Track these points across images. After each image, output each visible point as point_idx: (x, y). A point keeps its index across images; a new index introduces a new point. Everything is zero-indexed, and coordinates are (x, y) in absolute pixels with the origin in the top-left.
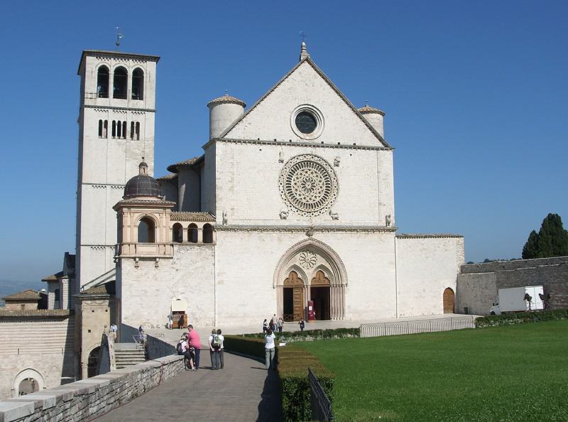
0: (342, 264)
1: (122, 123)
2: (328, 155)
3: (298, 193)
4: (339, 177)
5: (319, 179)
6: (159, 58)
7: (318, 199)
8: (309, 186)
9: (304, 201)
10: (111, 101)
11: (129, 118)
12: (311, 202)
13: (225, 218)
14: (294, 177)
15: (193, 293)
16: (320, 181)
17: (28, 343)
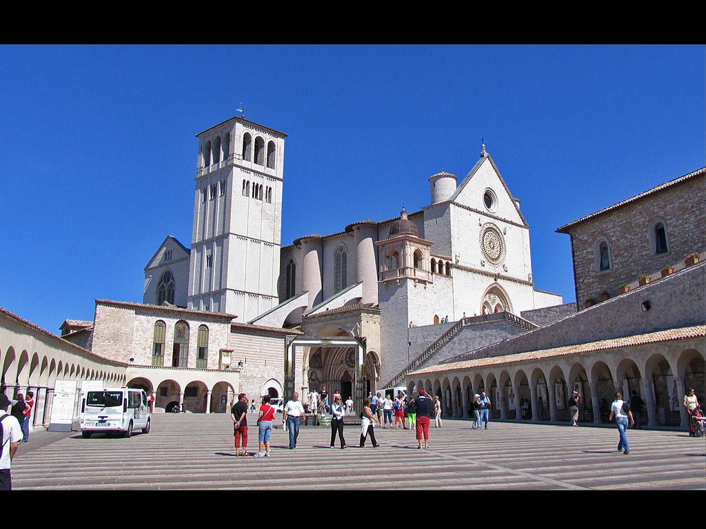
10: (250, 164)
11: (265, 182)
13: (458, 259)
14: (485, 238)
17: (273, 356)
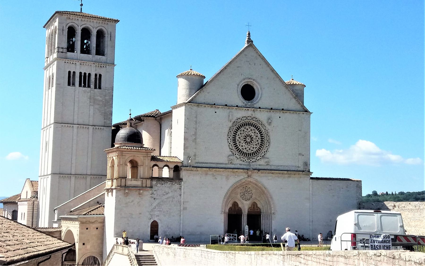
0: (271, 198)
1: (87, 75)
3: (241, 144)
4: (271, 134)
5: (256, 135)
6: (118, 21)
7: (255, 150)
9: (245, 151)
12: (250, 152)
14: (239, 133)
15: (165, 216)
16: (257, 136)
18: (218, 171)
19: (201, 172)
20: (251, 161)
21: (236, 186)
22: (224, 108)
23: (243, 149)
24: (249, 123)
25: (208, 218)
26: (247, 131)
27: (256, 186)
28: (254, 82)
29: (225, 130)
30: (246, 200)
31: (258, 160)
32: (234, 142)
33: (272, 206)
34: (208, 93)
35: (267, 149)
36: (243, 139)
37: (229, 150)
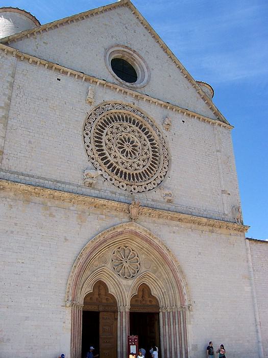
0: (182, 272)
2: (154, 113)
4: (170, 145)
5: (143, 142)
7: (141, 170)
8: (127, 147)
9: (121, 168)
14: (107, 130)
18: (59, 198)
19: (12, 194)
20: (134, 189)
21: (102, 239)
22: (76, 77)
23: (117, 163)
24: (129, 118)
25: (27, 318)
26: (123, 130)
27: (147, 245)
28: (134, 55)
29: (78, 116)
30: (126, 278)
31: (149, 190)
32: (96, 146)
33: (184, 291)
34: (46, 43)
35: (166, 172)
36: (117, 144)
37: (87, 158)
